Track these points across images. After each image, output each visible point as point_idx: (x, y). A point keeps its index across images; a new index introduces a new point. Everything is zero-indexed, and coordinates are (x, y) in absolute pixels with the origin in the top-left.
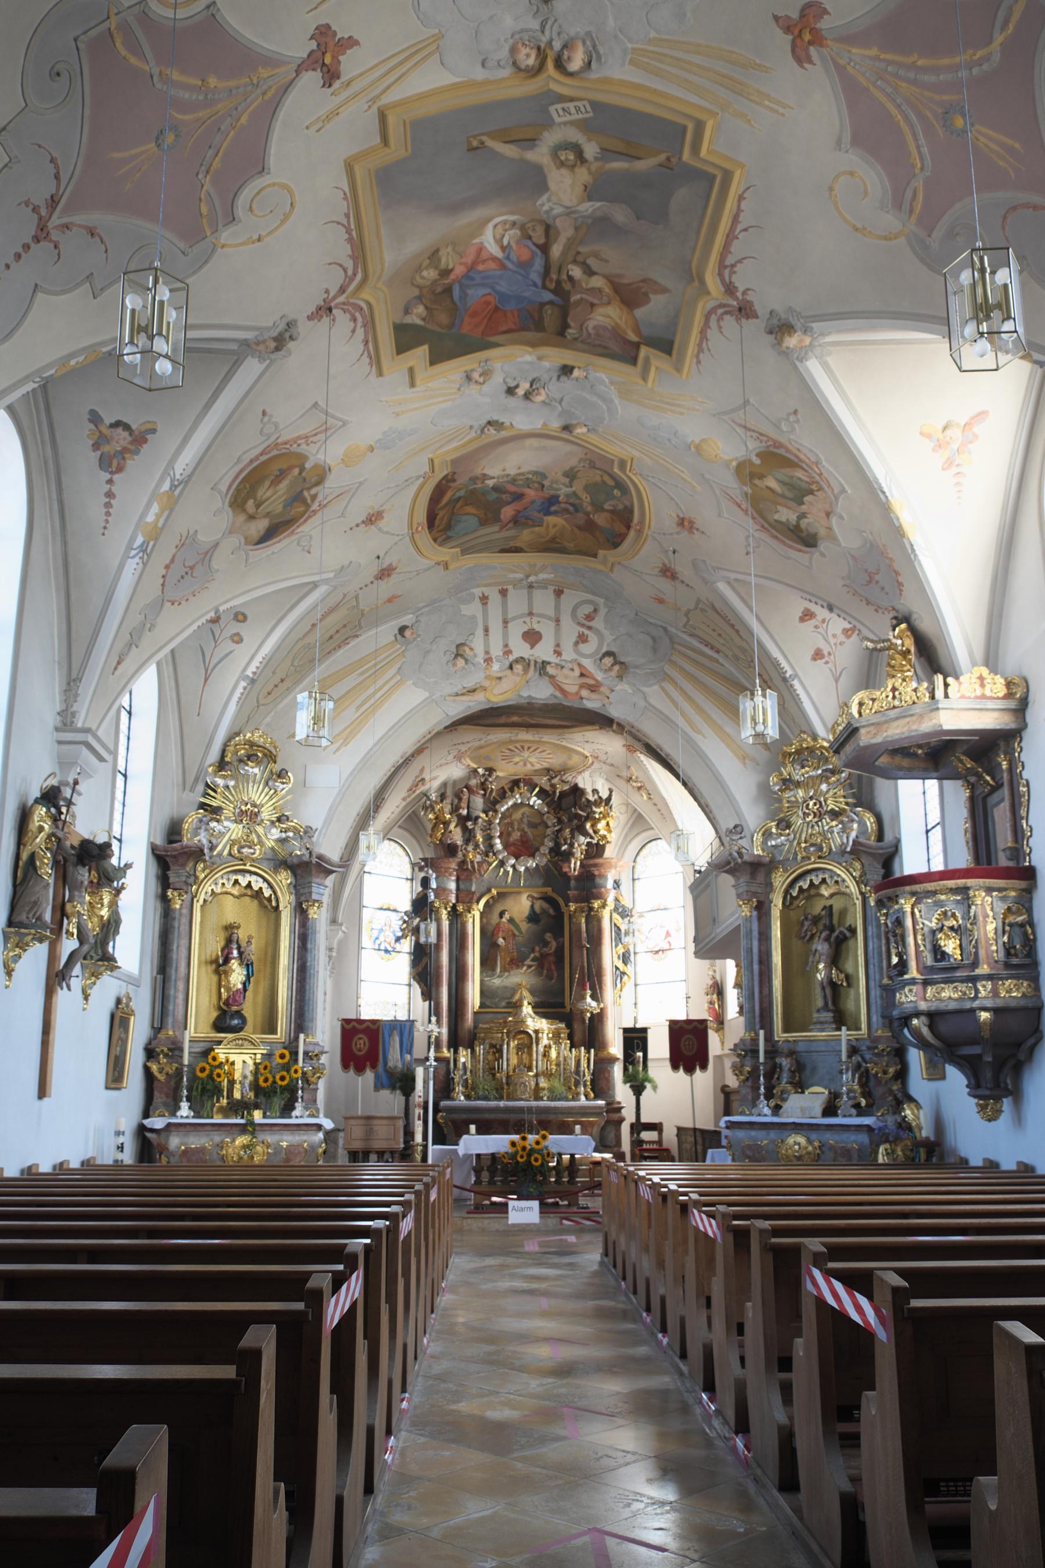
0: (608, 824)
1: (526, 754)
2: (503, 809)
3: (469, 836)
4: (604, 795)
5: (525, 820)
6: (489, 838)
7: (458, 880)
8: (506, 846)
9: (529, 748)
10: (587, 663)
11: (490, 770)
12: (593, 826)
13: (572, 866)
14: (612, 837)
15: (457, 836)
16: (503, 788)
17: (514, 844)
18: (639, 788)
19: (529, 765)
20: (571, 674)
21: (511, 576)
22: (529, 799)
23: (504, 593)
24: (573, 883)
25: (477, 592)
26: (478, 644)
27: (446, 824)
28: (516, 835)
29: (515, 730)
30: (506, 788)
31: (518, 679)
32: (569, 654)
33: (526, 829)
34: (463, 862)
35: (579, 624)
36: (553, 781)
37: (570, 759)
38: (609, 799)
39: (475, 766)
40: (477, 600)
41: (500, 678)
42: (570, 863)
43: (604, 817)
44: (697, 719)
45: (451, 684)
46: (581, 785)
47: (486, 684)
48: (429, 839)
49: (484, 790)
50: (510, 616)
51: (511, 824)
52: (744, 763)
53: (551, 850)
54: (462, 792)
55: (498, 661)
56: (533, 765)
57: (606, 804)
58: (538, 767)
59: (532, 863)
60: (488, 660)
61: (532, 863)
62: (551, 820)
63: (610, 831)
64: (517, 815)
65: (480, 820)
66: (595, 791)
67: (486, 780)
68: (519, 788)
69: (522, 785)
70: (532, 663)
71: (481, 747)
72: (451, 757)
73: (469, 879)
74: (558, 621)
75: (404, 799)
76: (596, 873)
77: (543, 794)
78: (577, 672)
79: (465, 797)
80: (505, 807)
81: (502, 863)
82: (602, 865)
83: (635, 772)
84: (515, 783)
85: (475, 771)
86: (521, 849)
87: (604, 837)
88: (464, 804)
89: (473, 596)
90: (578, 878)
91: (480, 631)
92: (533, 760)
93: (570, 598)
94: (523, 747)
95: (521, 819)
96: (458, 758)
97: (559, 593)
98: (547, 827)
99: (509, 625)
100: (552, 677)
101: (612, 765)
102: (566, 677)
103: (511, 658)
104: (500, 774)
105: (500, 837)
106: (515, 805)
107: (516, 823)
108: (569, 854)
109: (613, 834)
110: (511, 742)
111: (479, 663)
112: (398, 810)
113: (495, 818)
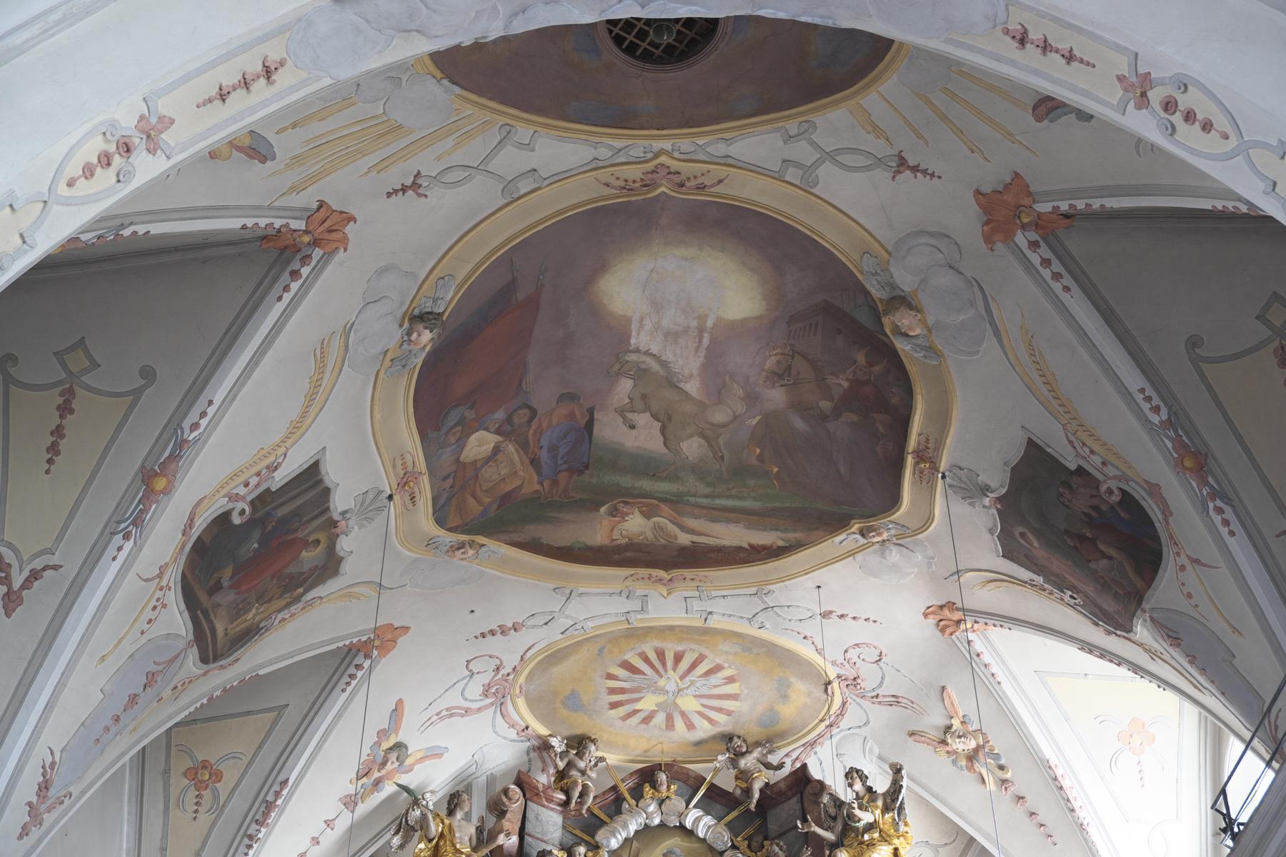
1: (670, 681)
2: (614, 844)
4: (881, 784)
9: (678, 658)
11: (579, 743)
16: (614, 788)
18: (972, 757)
19: (679, 724)
29: (642, 582)
30: (623, 788)
37: (785, 697)
38: (896, 788)
39: (544, 731)
43: (885, 839)
46: (815, 773)
49: (567, 792)
54: (506, 791)
56: (690, 726)
57: (886, 809)
58: (704, 730)
66: (852, 774)
67: (570, 765)
68: (655, 786)
69: (662, 777)
71: (555, 657)
72: (475, 689)
75: (350, 802)
77: (716, 799)
79: (515, 807)
83: (962, 703)
84: (647, 776)
85: (544, 746)
88: (511, 823)
92: (689, 704)
94: (661, 655)
96: (497, 694)
101: (895, 701)
104: (612, 759)
106: (646, 832)
110: (634, 634)
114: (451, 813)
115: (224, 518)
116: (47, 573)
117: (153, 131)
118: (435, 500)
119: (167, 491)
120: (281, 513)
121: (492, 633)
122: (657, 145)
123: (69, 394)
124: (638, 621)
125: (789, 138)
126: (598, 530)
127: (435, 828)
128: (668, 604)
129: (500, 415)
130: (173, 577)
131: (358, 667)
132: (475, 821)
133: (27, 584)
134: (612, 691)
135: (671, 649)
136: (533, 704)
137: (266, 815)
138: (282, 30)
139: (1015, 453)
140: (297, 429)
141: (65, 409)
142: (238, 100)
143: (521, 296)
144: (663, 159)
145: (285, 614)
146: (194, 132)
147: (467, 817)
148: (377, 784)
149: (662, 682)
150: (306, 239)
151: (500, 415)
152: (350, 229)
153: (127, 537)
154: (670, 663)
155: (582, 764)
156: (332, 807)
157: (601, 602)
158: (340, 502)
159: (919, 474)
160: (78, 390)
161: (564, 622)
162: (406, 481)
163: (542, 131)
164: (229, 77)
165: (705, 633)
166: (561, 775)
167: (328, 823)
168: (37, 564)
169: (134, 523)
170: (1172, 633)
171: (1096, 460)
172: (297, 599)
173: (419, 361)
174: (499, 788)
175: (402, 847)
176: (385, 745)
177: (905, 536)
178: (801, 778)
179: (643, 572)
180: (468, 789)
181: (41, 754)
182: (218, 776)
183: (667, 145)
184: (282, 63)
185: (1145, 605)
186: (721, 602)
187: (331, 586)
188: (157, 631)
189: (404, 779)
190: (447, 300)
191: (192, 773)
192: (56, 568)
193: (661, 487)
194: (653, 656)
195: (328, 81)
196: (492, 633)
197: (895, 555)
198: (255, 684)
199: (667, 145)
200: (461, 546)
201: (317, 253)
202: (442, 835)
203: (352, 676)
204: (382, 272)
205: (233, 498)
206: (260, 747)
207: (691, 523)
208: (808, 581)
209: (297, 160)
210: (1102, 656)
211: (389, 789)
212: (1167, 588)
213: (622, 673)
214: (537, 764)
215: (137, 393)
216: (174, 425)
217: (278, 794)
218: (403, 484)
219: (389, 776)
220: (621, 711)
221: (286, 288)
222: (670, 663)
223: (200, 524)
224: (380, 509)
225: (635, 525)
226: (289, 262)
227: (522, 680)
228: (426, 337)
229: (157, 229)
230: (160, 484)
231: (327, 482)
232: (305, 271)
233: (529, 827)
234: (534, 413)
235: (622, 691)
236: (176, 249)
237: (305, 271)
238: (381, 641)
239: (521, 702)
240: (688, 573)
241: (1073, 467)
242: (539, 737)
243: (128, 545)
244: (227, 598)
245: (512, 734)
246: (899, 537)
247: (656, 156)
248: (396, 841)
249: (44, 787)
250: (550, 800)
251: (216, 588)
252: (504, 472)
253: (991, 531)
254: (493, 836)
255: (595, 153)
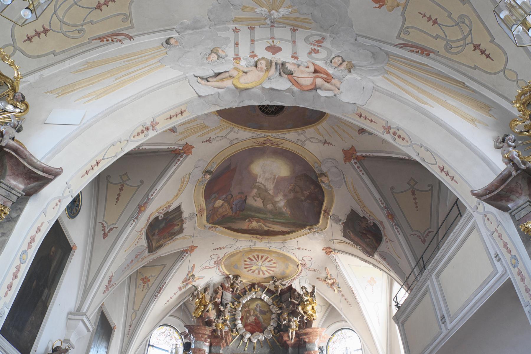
0: (313, 308)
1: (260, 263)
2: (244, 302)
3: (220, 313)
4: (310, 290)
5: (258, 309)
6: (234, 320)
7: (211, 346)
8: (245, 326)
9: (262, 257)
10: (321, 64)
11: (236, 277)
12: (303, 309)
13: (290, 334)
14: (317, 316)
15: (212, 315)
17: (250, 324)
18: (332, 285)
19: (261, 273)
20: (307, 69)
21: (259, 10)
22: (261, 296)
23: (252, 29)
24: (290, 349)
25: (232, 26)
26: (230, 51)
27: (206, 306)
28: (252, 319)
30: (247, 288)
31: (261, 74)
32: (303, 58)
33: (258, 315)
34: (215, 331)
35: (311, 44)
36: (276, 284)
37: (287, 268)
38: (313, 291)
39: (228, 273)
40: (231, 30)
41: (246, 73)
42: (288, 333)
43: (310, 304)
44: (421, 96)
45: (204, 69)
46: (294, 287)
47: (235, 73)
48: (193, 315)
49: (233, 289)
50: (255, 39)
51: (249, 311)
52: (475, 125)
53: (275, 328)
54: (218, 288)
55: (245, 59)
56: (264, 274)
57: (311, 296)
58: (267, 275)
59: (262, 337)
60: (237, 58)
61: (262, 337)
62: (275, 310)
63: (315, 313)
64: (253, 306)
65: (229, 305)
66: (303, 288)
67: (234, 282)
68: (254, 288)
69: (256, 286)
70: (274, 64)
71: (232, 255)
72: (212, 262)
73: (218, 345)
74: (294, 42)
75: (180, 289)
76: (307, 340)
77: (269, 292)
78: (312, 69)
79: (220, 292)
80: (246, 300)
81: (242, 337)
82: (311, 333)
84: (253, 286)
85: (228, 277)
86: (256, 327)
87: (312, 315)
88: (219, 295)
89: (229, 29)
90: (294, 346)
91: (232, 44)
92: (264, 268)
93: (301, 34)
94: (258, 256)
95: (256, 308)
96: (217, 264)
97: (294, 30)
98: (272, 313)
99: (255, 43)
100: (291, 73)
101: (314, 270)
102: (302, 72)
103: (256, 59)
104: (244, 281)
105: (241, 319)
107: (252, 311)
108: (288, 327)
109: (317, 314)
110: (252, 251)
111: (229, 60)
112: (175, 297)
113: (239, 307)
114: (205, 292)
115: (157, 218)
116: (114, 229)
117: (154, 126)
118: (207, 216)
119: (144, 210)
120: (170, 217)
121: (218, 249)
122: (268, 134)
123: (122, 186)
124: (253, 248)
125: (299, 134)
126: (245, 225)
127: (201, 296)
128: (261, 244)
129: (224, 196)
130: (144, 231)
131: (185, 256)
132: (210, 294)
133: (109, 231)
134: (245, 264)
135: (261, 255)
136: (226, 266)
137: (160, 291)
138: (186, 103)
139: (348, 212)
140: (176, 197)
141: (121, 189)
142: (174, 119)
143: (232, 168)
144: (269, 137)
145: (169, 242)
146: (164, 126)
147: (208, 294)
148: (187, 284)
149: (258, 263)
150: (182, 152)
151: (224, 196)
152: (193, 150)
153: (134, 221)
154: (260, 258)
155: (237, 282)
156: (176, 290)
157: (244, 243)
158: (185, 215)
159: (324, 216)
160: (125, 185)
161: (235, 247)
162: (201, 211)
163: (241, 129)
164: (173, 114)
165: (269, 252)
166: (232, 284)
167: (175, 294)
168: (112, 227)
169: (136, 218)
170: (384, 257)
171: (368, 215)
172: (172, 238)
173: (206, 182)
174: (216, 287)
175: (192, 300)
176: (190, 275)
177: (319, 231)
178: (290, 288)
179: (255, 236)
180: (209, 287)
181: (109, 274)
182: (149, 281)
183: (270, 134)
184: (185, 111)
185: (378, 250)
186: (273, 244)
187: (181, 236)
188: (138, 245)
189: (193, 284)
190: (214, 168)
191: (142, 280)
192: (116, 228)
193: (261, 216)
194: (256, 257)
195: (195, 116)
196: (218, 249)
197: (317, 235)
198: (160, 258)
199: (270, 134)
200: (212, 227)
201: (185, 155)
202: (202, 298)
203: (183, 258)
204: (199, 160)
205: (160, 213)
206: (159, 274)
207: (268, 225)
208: (295, 240)
209: (182, 133)
210: (365, 262)
211: (190, 286)
212: (383, 247)
213: (248, 260)
214: (226, 281)
215: (139, 186)
216: (147, 194)
217: (163, 286)
218: (200, 212)
219: (190, 283)
220: (247, 269)
221: (176, 163)
222: (260, 258)
223: (151, 219)
224: (194, 218)
225: (254, 224)
226: (177, 157)
227: (224, 261)
228: (208, 176)
229: (148, 147)
230: (143, 209)
231: (182, 210)
232: (181, 159)
233: (223, 297)
234: (232, 196)
235: (248, 265)
236: (151, 152)
237: (181, 159)
238: (192, 249)
239: (223, 266)
240: (266, 237)
241: (362, 216)
242: (227, 275)
243: (134, 223)
244: (156, 237)
245: (220, 274)
246: (318, 231)
247: (267, 136)
248: (191, 299)
249: (110, 281)
250: (229, 290)
251: (154, 235)
252: (224, 210)
253: (341, 230)
254: (214, 299)
255: (253, 135)
